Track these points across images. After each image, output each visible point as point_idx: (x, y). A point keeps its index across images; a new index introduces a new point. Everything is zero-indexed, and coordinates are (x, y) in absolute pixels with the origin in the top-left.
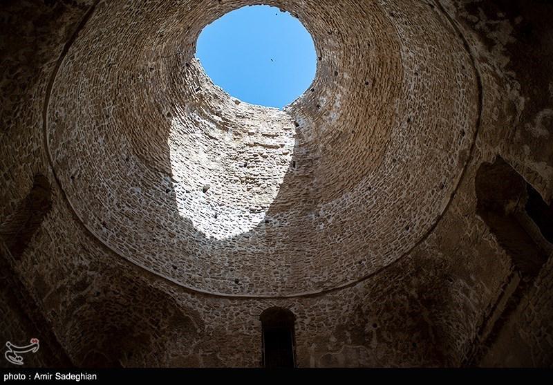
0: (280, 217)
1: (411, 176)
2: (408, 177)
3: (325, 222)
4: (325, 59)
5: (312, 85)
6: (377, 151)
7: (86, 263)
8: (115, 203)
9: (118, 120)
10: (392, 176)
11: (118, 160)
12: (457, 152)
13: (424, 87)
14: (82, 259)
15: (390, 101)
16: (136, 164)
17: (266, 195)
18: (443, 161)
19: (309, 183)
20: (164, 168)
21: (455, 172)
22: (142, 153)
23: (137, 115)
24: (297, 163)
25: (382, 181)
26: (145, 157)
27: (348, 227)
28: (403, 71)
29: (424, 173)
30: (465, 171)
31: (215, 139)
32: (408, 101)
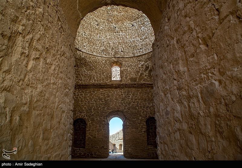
7: (143, 63)
8: (139, 40)
14: (141, 63)
16: (136, 22)
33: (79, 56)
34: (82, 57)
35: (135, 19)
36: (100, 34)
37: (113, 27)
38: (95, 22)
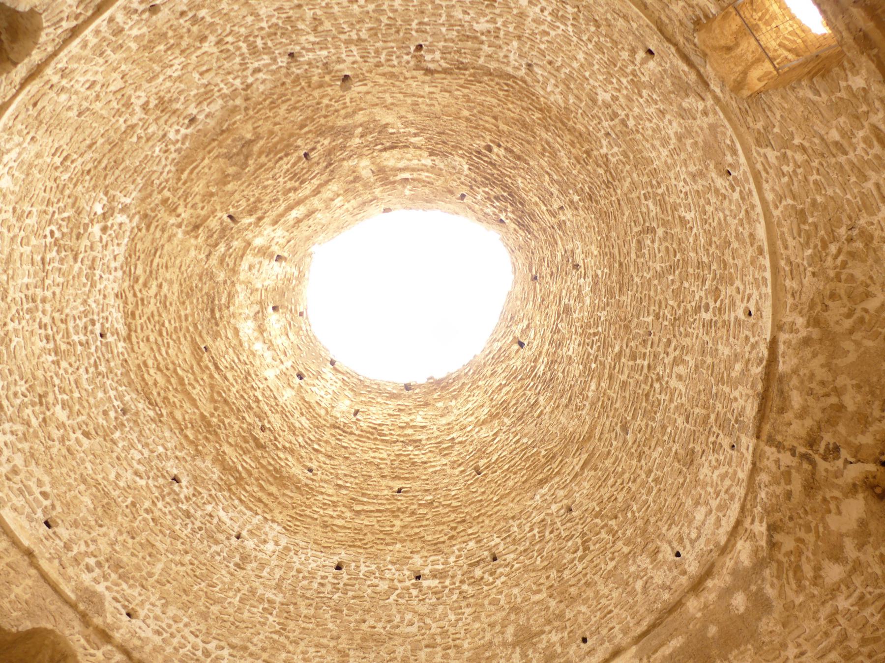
0: (179, 145)
1: (84, 440)
2: (86, 435)
3: (101, 218)
4: (328, 370)
5: (307, 318)
6: (156, 383)
9: (584, 130)
10: (100, 395)
11: (550, 63)
12: (100, 588)
13: (217, 542)
15: (220, 460)
16: (508, 64)
17: (235, 150)
18: (94, 541)
19: (185, 222)
20: (448, 77)
21: (70, 571)
22: (507, 85)
23: (551, 140)
24: (232, 225)
25: (102, 368)
26: (496, 79)
27: (62, 261)
28: (251, 509)
29: (84, 481)
30: (66, 601)
31: (385, 149)
32: (205, 494)
33: (807, 352)
34: (803, 333)
35: (500, 76)
36: (676, 210)
37: (616, 149)
38: (646, 251)
